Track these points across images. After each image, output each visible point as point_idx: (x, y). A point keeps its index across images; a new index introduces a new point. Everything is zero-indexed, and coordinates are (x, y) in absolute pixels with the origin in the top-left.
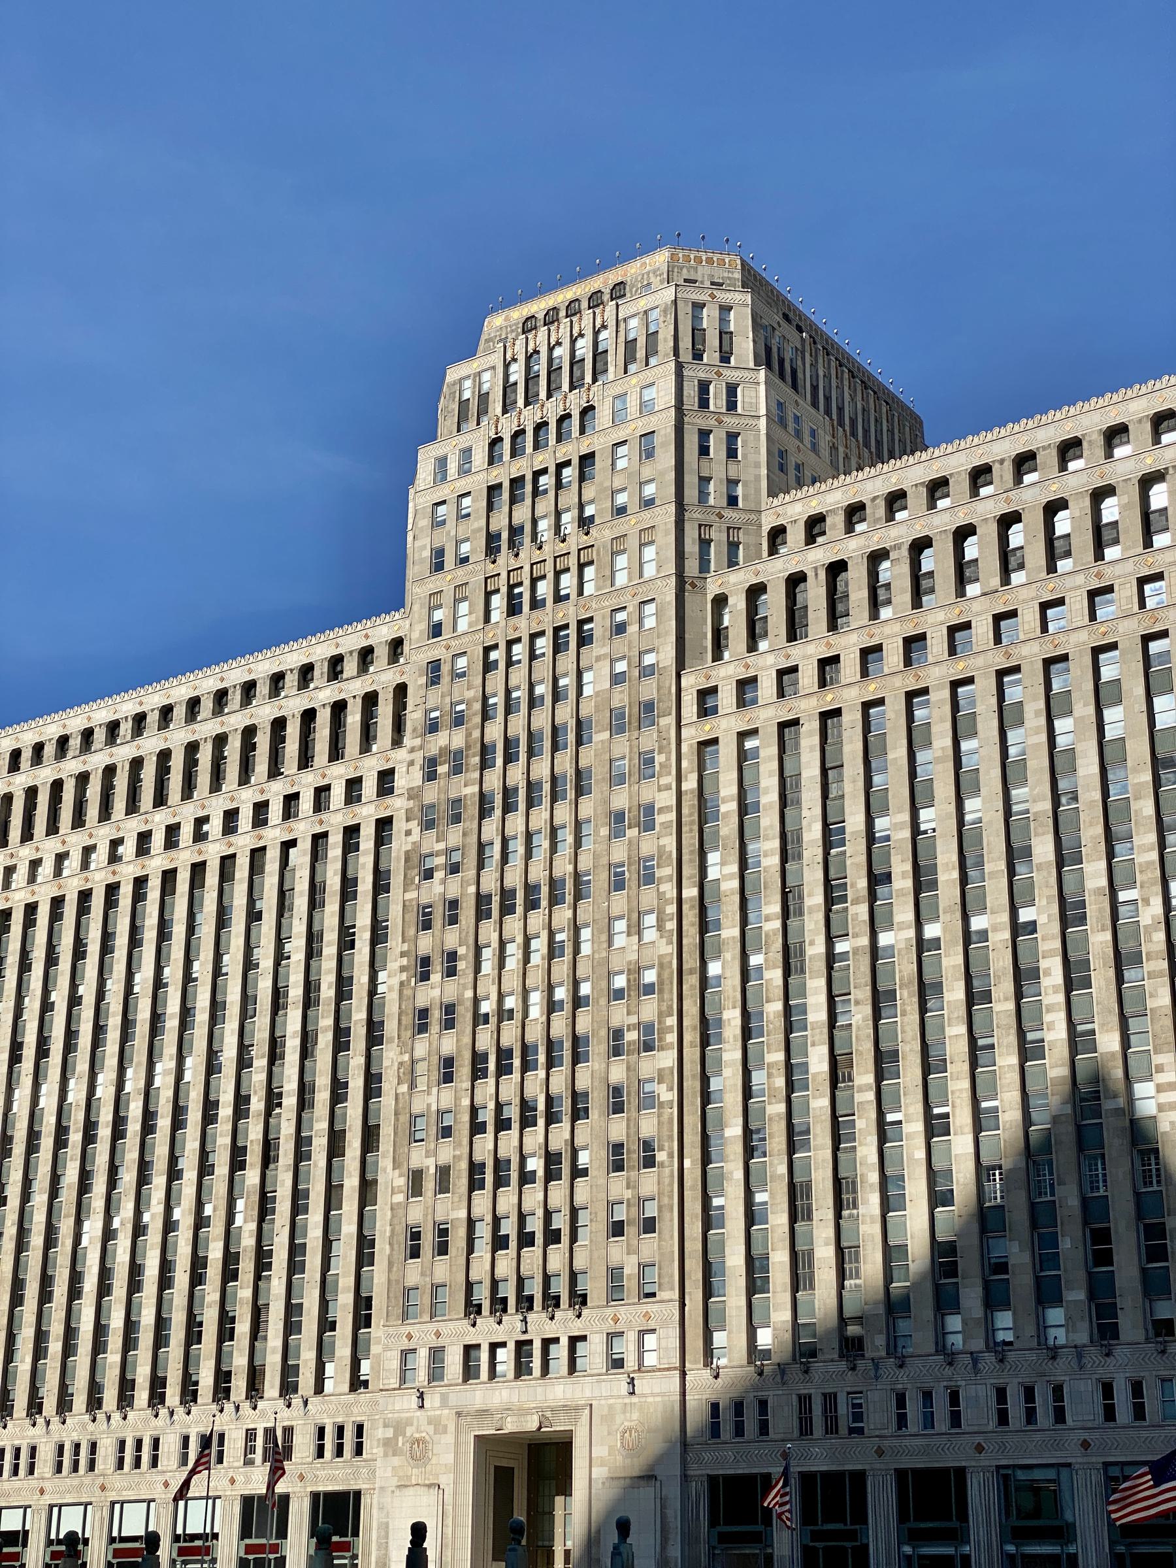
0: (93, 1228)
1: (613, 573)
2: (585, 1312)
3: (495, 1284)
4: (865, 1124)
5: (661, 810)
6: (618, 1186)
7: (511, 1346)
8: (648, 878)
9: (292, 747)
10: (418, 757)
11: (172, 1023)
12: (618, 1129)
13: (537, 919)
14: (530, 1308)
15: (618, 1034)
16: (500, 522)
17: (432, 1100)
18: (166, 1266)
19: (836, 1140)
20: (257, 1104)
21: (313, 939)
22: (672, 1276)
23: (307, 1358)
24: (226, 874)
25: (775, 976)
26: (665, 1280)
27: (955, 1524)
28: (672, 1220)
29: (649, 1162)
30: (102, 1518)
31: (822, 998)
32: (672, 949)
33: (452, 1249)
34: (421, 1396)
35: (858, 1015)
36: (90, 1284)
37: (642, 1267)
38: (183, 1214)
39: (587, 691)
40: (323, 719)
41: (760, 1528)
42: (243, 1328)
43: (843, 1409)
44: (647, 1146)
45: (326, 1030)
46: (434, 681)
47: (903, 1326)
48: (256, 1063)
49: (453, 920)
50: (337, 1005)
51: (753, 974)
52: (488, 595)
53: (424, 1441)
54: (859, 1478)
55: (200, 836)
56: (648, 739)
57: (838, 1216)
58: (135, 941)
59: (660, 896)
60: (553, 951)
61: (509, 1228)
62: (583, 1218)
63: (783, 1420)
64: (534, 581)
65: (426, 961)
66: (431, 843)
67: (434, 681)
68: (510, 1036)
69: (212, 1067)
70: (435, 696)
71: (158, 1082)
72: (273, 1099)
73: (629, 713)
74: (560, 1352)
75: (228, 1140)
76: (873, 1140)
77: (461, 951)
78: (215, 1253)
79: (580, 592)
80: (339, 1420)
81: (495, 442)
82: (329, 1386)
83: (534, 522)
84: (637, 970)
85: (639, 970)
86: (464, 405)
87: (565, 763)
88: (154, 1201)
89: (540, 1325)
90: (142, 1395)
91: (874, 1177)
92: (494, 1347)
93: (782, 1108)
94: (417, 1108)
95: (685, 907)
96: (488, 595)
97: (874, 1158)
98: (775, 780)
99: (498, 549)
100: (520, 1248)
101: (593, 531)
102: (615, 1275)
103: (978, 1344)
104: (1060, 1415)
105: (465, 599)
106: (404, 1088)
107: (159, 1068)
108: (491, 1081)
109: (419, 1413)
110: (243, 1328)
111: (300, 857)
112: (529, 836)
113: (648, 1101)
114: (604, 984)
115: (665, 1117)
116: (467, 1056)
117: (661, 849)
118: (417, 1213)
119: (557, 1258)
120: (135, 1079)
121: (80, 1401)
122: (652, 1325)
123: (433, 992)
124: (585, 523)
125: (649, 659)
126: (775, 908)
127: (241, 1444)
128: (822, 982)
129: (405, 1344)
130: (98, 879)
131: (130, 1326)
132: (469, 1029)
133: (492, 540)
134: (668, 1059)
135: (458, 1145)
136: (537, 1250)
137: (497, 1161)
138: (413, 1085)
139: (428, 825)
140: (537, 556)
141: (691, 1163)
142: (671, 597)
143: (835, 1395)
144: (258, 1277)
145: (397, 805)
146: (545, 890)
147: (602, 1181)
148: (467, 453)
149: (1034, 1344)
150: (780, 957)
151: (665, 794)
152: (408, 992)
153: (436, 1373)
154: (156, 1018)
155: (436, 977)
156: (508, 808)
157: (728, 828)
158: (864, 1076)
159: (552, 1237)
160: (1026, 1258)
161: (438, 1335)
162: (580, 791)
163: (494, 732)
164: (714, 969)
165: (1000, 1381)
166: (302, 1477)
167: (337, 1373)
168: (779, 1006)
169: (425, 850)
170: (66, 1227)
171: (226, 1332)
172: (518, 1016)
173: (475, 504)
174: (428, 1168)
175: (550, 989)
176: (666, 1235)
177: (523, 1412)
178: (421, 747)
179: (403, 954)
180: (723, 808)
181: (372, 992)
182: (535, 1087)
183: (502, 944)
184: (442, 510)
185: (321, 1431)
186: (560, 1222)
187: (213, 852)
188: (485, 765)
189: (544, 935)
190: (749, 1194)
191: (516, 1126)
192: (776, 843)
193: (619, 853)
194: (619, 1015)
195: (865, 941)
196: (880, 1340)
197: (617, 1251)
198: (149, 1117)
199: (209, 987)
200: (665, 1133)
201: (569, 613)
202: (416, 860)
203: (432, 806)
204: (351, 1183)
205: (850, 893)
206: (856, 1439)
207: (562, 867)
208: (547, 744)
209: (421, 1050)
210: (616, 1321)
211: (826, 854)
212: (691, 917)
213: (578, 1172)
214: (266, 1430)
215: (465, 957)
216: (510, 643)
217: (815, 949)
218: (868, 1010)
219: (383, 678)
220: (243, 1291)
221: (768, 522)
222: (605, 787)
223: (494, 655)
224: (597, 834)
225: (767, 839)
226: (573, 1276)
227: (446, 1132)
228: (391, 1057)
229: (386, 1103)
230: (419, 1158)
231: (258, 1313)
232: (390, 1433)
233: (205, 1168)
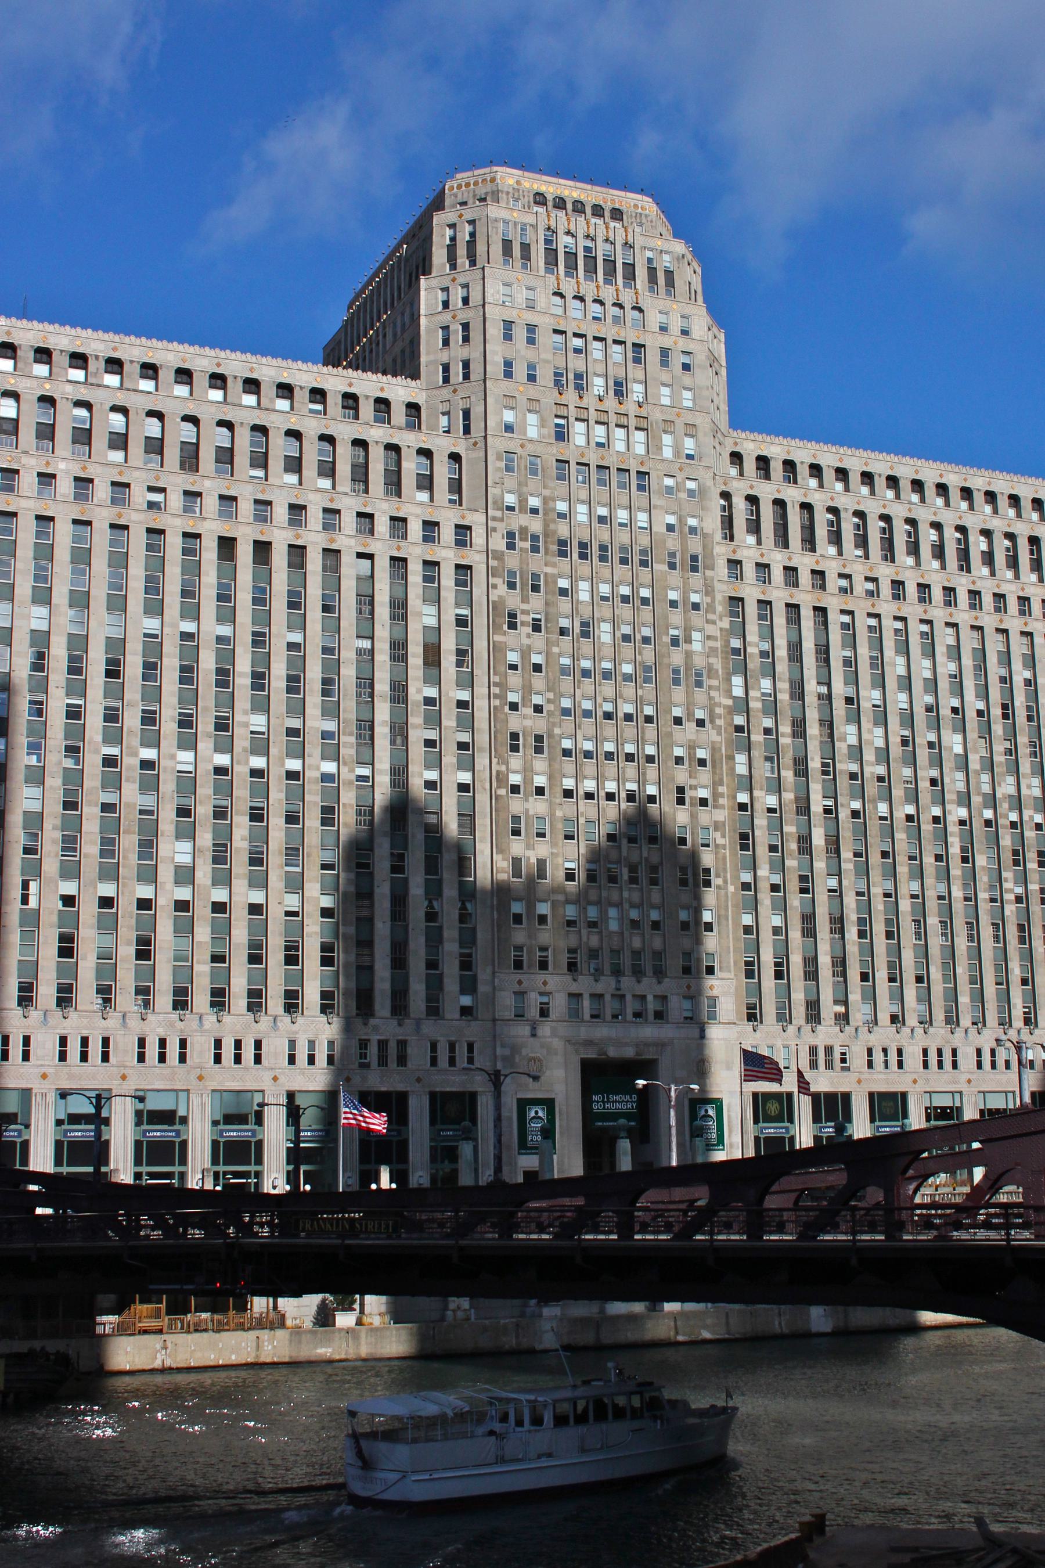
22: (729, 962)
26: (724, 965)
28: (728, 926)
43: (837, 1056)
47: (895, 1009)
53: (540, 1060)
54: (846, 1097)
80: (453, 1039)
109: (532, 1039)
115: (720, 856)
129: (517, 988)
135: (554, 844)
143: (832, 1047)
165: (925, 1045)
174: (528, 858)
179: (496, 684)
194: (681, 775)
214: (379, 1042)
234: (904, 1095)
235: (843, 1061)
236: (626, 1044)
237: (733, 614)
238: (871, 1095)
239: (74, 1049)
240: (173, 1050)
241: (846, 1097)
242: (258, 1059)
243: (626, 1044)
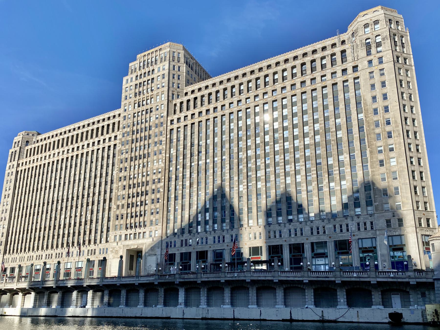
0: (63, 217)
1: (156, 99)
2: (146, 228)
3: (131, 224)
4: (195, 194)
5: (163, 141)
6: (153, 206)
8: (161, 153)
9: (100, 132)
10: (121, 133)
11: (77, 181)
12: (153, 196)
13: (141, 161)
14: (137, 227)
15: (154, 180)
16: (137, 91)
17: (121, 193)
18: (75, 223)
19: (190, 197)
20: (91, 195)
21: (102, 166)
24: (87, 155)
25: (181, 169)
27: (205, 260)
29: (158, 202)
31: (189, 173)
32: (164, 165)
33: (124, 218)
34: (117, 243)
36: (62, 226)
37: (156, 220)
38: (78, 214)
39: (151, 121)
40: (106, 127)
41: (173, 262)
42: (88, 233)
45: (103, 181)
46: (125, 119)
48: (91, 188)
49: (126, 161)
50: (106, 177)
51: (178, 169)
52: (135, 104)
53: (117, 250)
54: (190, 253)
55: (83, 148)
56: (161, 129)
57: (190, 210)
58: (71, 167)
59: (162, 156)
60: (144, 166)
61: (134, 214)
62: (146, 212)
64: (143, 101)
65: (121, 169)
66: (123, 148)
67: (125, 119)
68: (135, 181)
69: (84, 189)
70: (125, 122)
71: (74, 192)
72: (94, 194)
73: (159, 124)
74: (142, 235)
75: (86, 201)
76: (196, 197)
77: (128, 167)
78: (83, 220)
79: (151, 103)
81: (137, 76)
82: (102, 242)
83: (143, 90)
84: (158, 169)
85: (158, 169)
86: (132, 70)
87: (147, 133)
88: (73, 212)
89: (138, 230)
91: (196, 203)
92: (130, 234)
93: (181, 192)
94: (119, 194)
95: (167, 158)
96: (135, 104)
97: (196, 200)
98: (183, 135)
99: (137, 96)
100: (135, 217)
101: (153, 92)
102: (151, 221)
103: (211, 230)
104: (224, 241)
105: (130, 105)
106: (117, 191)
107: (75, 189)
108: (132, 189)
109: (117, 246)
110: (88, 233)
111: (100, 152)
112: (140, 146)
113: (159, 192)
114: (152, 172)
116: (128, 185)
117: (163, 148)
118: (118, 212)
122: (157, 229)
123: (122, 174)
124: (152, 90)
125: (162, 115)
126: (182, 158)
127: (87, 252)
128: (189, 170)
129: (115, 234)
130: (65, 156)
131: (69, 233)
132: (128, 180)
133: (136, 94)
134: (162, 184)
136: (138, 218)
137: (132, 203)
138: (118, 191)
139: (123, 145)
140: (143, 96)
141: (165, 202)
142: (166, 103)
144: (91, 224)
145: (117, 142)
146: (142, 156)
147: (150, 205)
148: (132, 78)
149: (220, 229)
150: (182, 166)
151: (164, 138)
152: (118, 174)
153: (120, 239)
154: (74, 181)
155: (123, 172)
156: (137, 142)
157: (174, 144)
158: (195, 186)
159: (141, 215)
161: (121, 233)
162: (149, 138)
163: (135, 128)
164: (171, 169)
166: (97, 257)
167: (104, 240)
168: (182, 174)
169: (122, 149)
170: (58, 217)
171: (85, 234)
172: (137, 178)
173: (133, 88)
175: (143, 173)
176: (160, 214)
177: (135, 245)
178: (122, 131)
179: (117, 168)
180: (174, 141)
181: (112, 175)
182: (139, 190)
183: (135, 165)
184: (127, 89)
186: (143, 213)
187: (85, 151)
188: (133, 134)
189: (142, 163)
190: (175, 207)
191: (136, 197)
192: (182, 146)
193: (156, 149)
194: (154, 177)
195: (197, 163)
196: (195, 230)
197: (152, 217)
198: (73, 198)
199: (84, 175)
200: (161, 197)
201: (149, 107)
202: (120, 151)
203: (123, 142)
204: (107, 208)
205: (195, 155)
206: (190, 247)
207: (146, 152)
208: (144, 130)
210: (151, 229)
211: (191, 148)
212: (167, 160)
213: (146, 204)
215: (128, 168)
216: (138, 112)
218: (196, 174)
219: (116, 120)
220: (88, 227)
221: (185, 91)
222: (154, 137)
223: (135, 115)
224: (152, 146)
225: (181, 146)
226: (144, 222)
227: (124, 198)
228: (115, 186)
229: (114, 194)
230: (119, 203)
231: (90, 231)
233: (82, 206)
234: (207, 251)
236: (135, 245)
238: (197, 252)
241: (190, 253)
243: (135, 245)
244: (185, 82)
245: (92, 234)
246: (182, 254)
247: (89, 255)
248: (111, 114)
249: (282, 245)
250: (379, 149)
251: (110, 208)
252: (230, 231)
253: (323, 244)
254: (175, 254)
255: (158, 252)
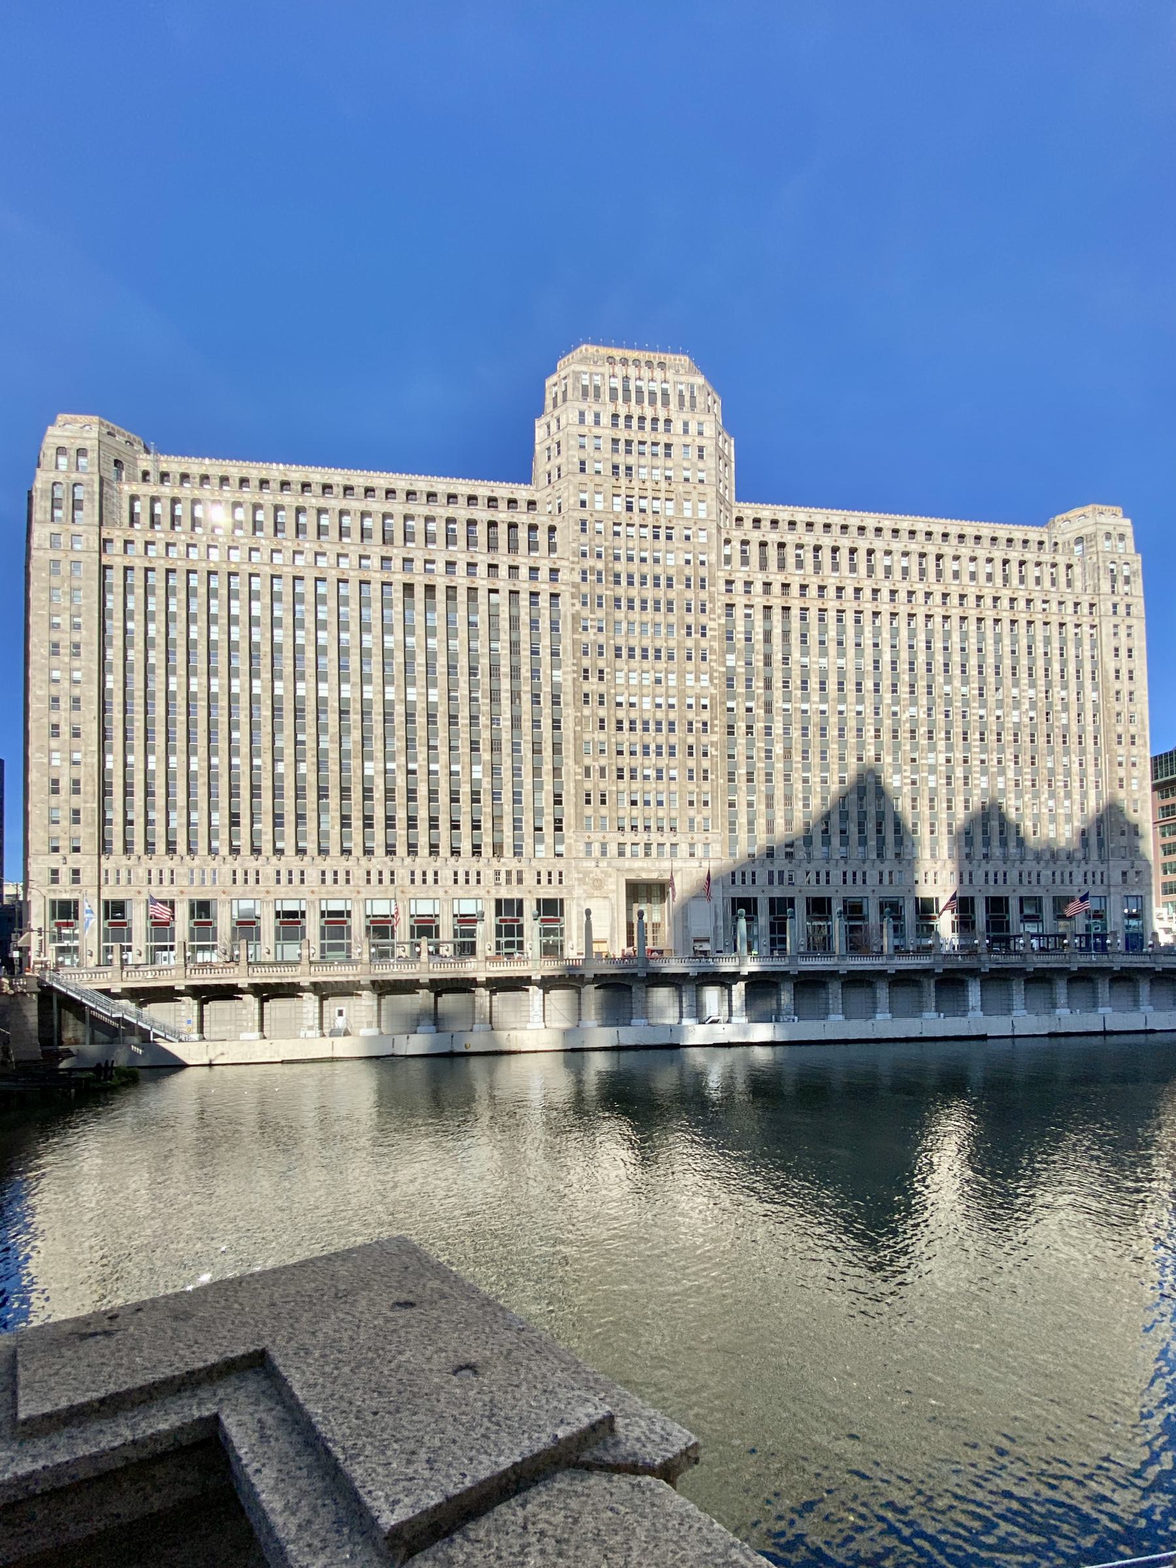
7: (642, 845)
12: (691, 763)
13: (646, 665)
15: (691, 724)
23: (528, 841)
30: (404, 907)
35: (796, 734)
42: (486, 824)
43: (786, 876)
44: (706, 771)
59: (711, 667)
63: (762, 879)
68: (634, 714)
74: (667, 848)
84: (698, 697)
90: (423, 850)
104: (864, 882)
113: (705, 754)
118: (588, 785)
119: (661, 813)
120: (396, 693)
121: (380, 851)
129: (587, 840)
135: (610, 758)
158: (797, 758)
160: (856, 829)
171: (476, 826)
185: (539, 874)
189: (652, 672)
193: (690, 643)
194: (691, 715)
197: (692, 812)
204: (547, 767)
209: (587, 711)
217: (778, 704)
227: (602, 751)
230: (587, 761)
232: (581, 876)
235: (791, 879)
236: (651, 871)
237: (728, 615)
239: (329, 877)
240: (386, 877)
242: (436, 881)
243: (651, 871)
244: (734, 488)
245: (505, 828)
246: (772, 900)
247: (499, 884)
248: (503, 490)
249: (972, 898)
250: (1120, 759)
251: (556, 772)
252: (878, 862)
253: (1037, 901)
254: (755, 899)
255: (717, 892)
